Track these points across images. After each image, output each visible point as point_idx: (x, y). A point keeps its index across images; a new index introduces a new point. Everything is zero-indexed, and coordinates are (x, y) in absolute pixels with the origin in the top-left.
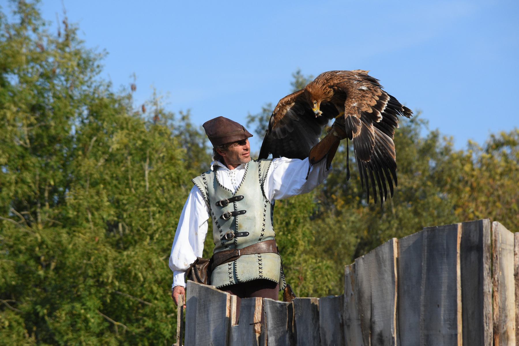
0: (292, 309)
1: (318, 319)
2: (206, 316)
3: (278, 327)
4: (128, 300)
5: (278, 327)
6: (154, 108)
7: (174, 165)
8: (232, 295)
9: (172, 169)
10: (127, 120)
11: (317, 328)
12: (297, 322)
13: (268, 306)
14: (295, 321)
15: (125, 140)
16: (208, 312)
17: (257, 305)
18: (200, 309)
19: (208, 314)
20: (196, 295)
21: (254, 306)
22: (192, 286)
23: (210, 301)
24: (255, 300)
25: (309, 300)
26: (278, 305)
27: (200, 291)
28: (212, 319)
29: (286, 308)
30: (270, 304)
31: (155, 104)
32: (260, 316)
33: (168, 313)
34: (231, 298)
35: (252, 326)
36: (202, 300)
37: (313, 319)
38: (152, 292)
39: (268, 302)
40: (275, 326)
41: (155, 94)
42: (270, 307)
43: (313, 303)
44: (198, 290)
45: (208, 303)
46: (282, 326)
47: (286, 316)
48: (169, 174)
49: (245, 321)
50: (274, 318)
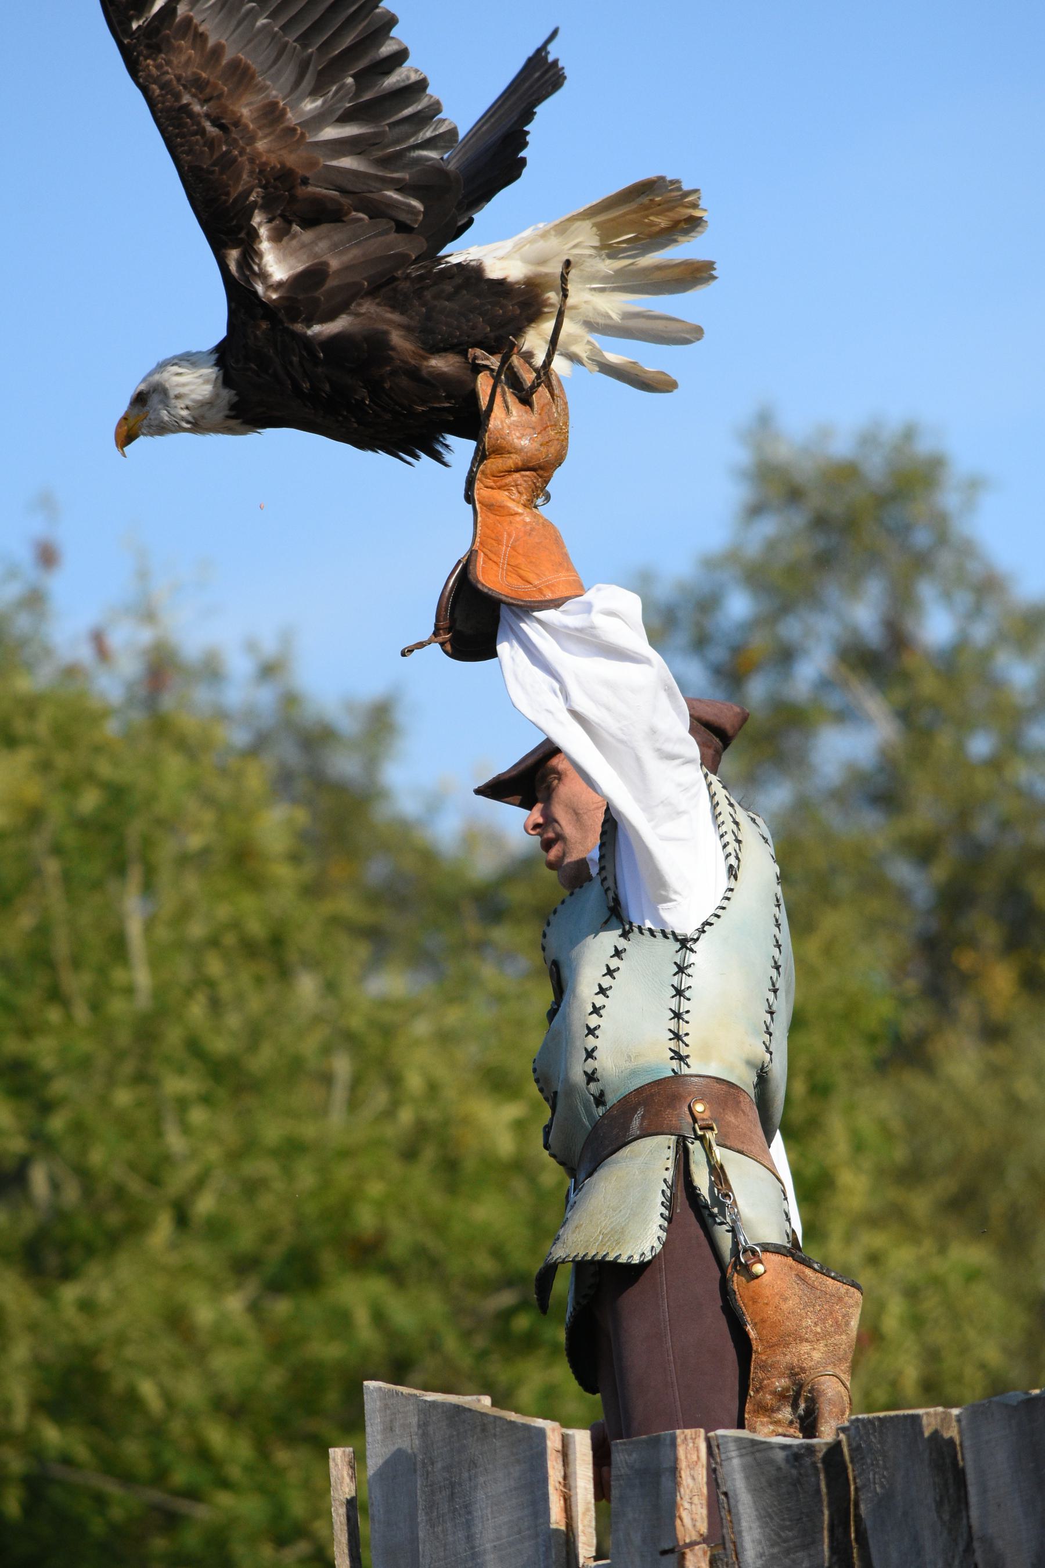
0: (846, 1468)
1: (962, 1500)
2: (461, 1534)
3: (787, 1552)
4: (100, 1500)
5: (787, 1552)
6: (145, 636)
7: (256, 883)
8: (570, 1432)
9: (248, 902)
10: (30, 707)
11: (961, 1548)
12: (868, 1523)
13: (736, 1462)
14: (858, 1516)
15: (33, 791)
16: (469, 1513)
17: (683, 1464)
18: (431, 1506)
19: (469, 1525)
20: (408, 1442)
21: (674, 1471)
22: (386, 1407)
23: (473, 1464)
24: (674, 1445)
25: (916, 1419)
26: (780, 1456)
27: (423, 1425)
28: (488, 1546)
29: (814, 1464)
30: (741, 1456)
31: (148, 615)
32: (702, 1511)
33: (281, 1541)
34: (565, 1441)
35: (672, 1558)
36: (439, 1465)
37: (939, 1504)
38: (204, 1455)
39: (732, 1446)
40: (775, 1550)
41: (143, 575)
42: (745, 1468)
43: (936, 1434)
44: (414, 1420)
45: (466, 1475)
46: (805, 1547)
47: (821, 1501)
48: (235, 925)
49: (637, 1538)
50: (765, 1517)
